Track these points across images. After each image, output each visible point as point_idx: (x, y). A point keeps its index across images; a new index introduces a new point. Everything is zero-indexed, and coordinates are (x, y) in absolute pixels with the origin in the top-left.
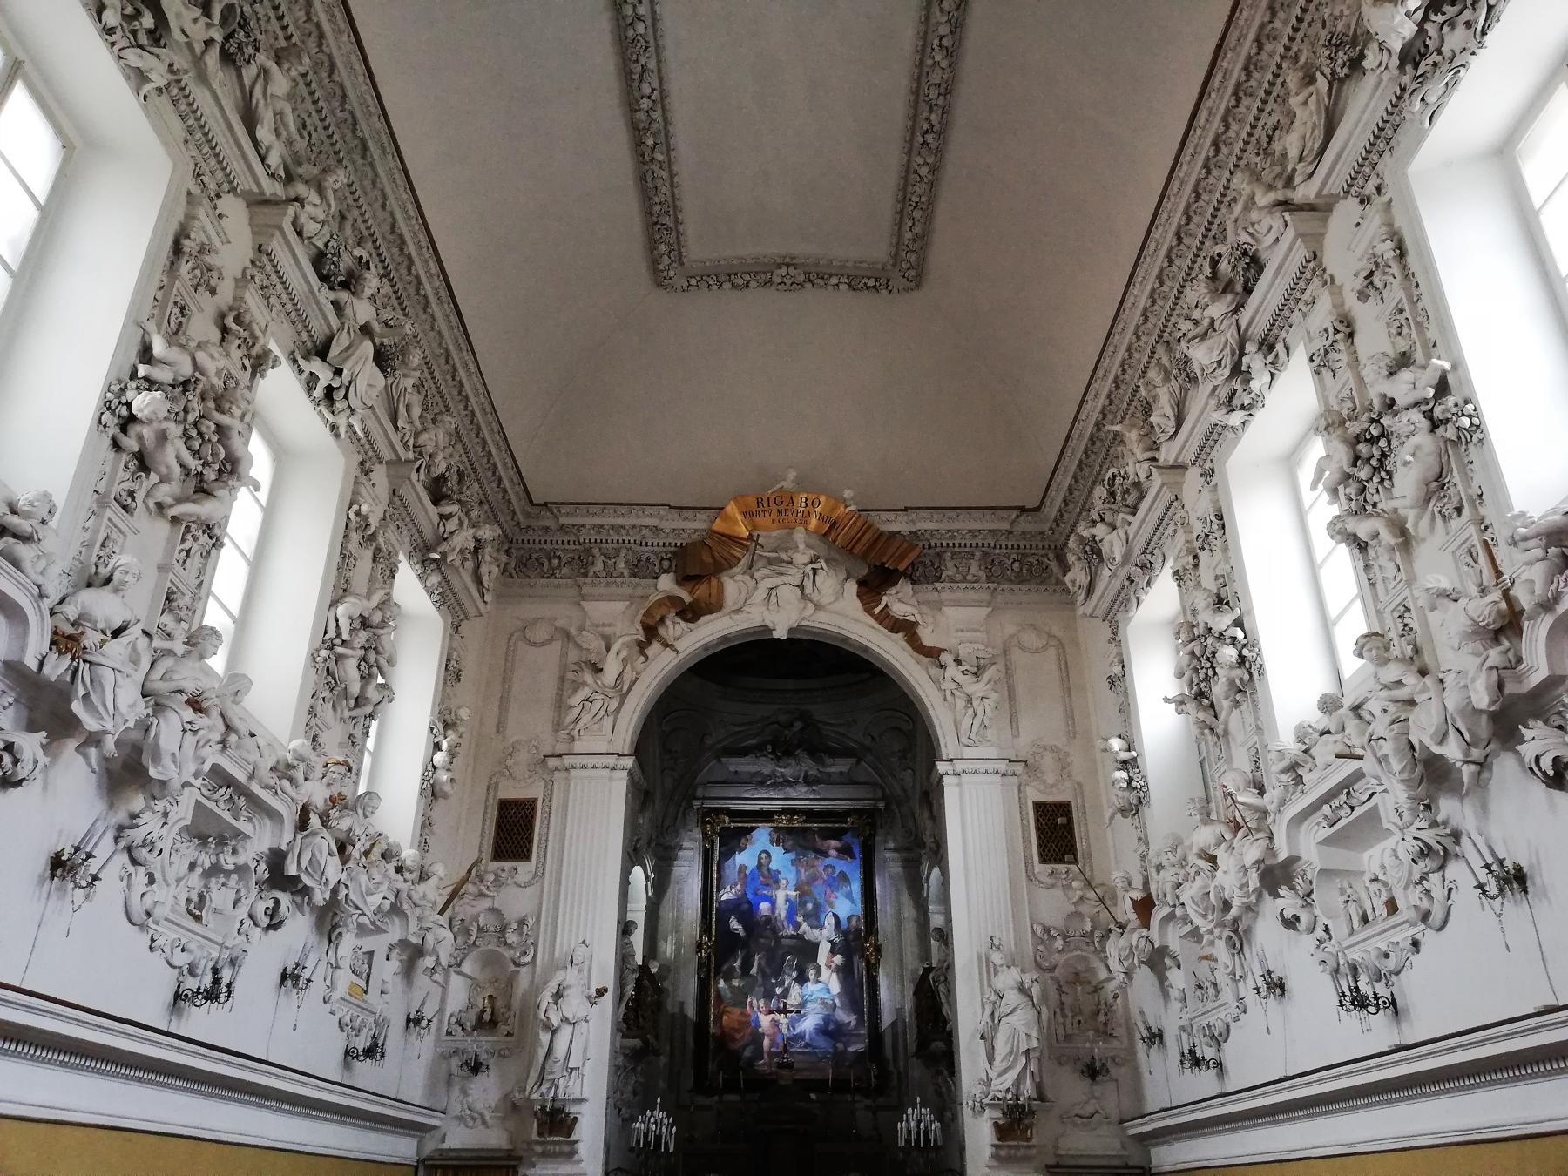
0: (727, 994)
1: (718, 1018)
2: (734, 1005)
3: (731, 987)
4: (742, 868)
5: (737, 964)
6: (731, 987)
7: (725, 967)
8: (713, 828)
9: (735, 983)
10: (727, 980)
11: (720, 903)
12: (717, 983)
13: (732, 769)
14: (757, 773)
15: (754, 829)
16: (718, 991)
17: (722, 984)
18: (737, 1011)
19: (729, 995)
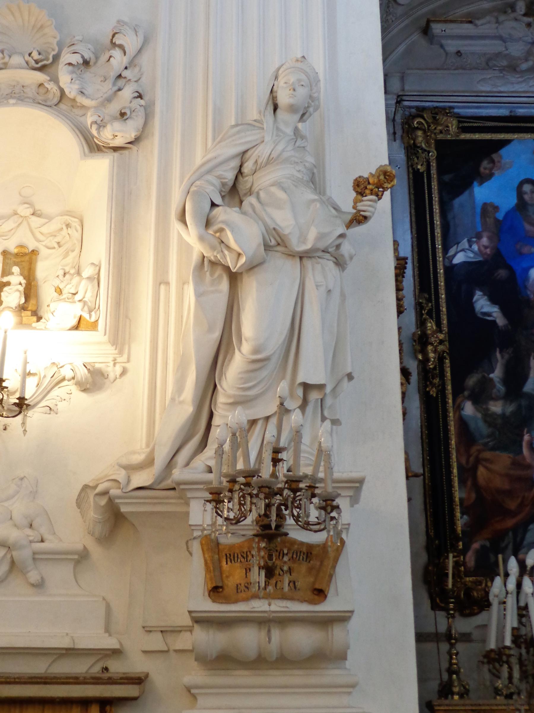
0: (480, 427)
1: (468, 473)
2: (504, 448)
3: (489, 418)
4: (488, 209)
5: (497, 374)
6: (489, 418)
7: (472, 381)
8: (426, 136)
9: (496, 408)
10: (479, 397)
11: (450, 269)
12: (459, 408)
13: (452, 46)
14: (498, 55)
15: (508, 142)
16: (462, 423)
17: (469, 409)
18: (503, 460)
19: (485, 430)
